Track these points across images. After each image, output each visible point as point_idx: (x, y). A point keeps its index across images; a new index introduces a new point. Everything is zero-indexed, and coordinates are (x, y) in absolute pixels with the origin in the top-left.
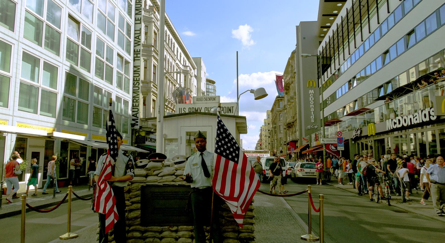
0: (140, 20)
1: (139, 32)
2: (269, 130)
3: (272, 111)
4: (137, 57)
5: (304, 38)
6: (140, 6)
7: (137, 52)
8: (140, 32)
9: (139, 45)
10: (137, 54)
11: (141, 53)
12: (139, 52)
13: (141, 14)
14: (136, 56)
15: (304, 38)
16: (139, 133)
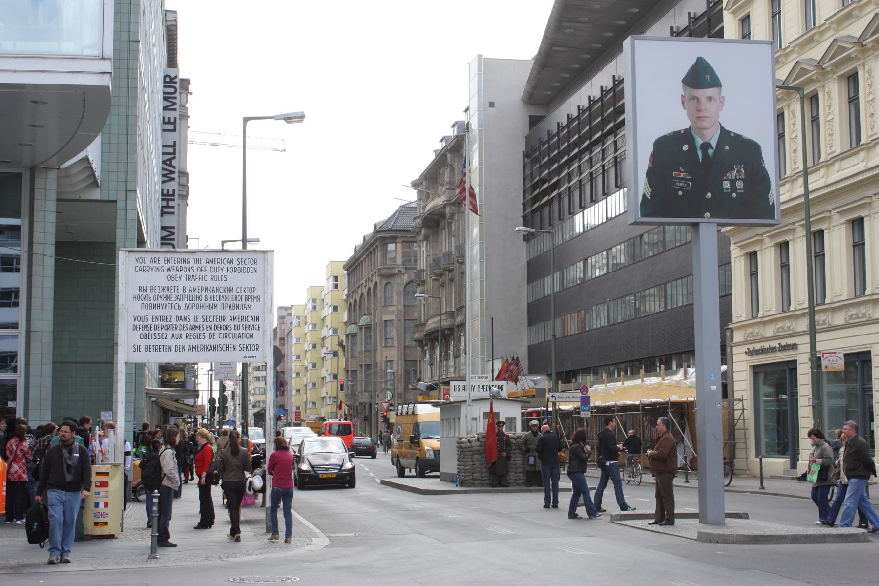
0: (174, 123)
1: (171, 150)
2: (335, 331)
3: (353, 266)
4: (168, 207)
5: (492, 105)
6: (172, 90)
7: (168, 194)
8: (175, 150)
9: (173, 179)
10: (168, 200)
11: (176, 197)
12: (173, 195)
13: (175, 110)
14: (165, 203)
15: (492, 105)
16: (170, 374)
